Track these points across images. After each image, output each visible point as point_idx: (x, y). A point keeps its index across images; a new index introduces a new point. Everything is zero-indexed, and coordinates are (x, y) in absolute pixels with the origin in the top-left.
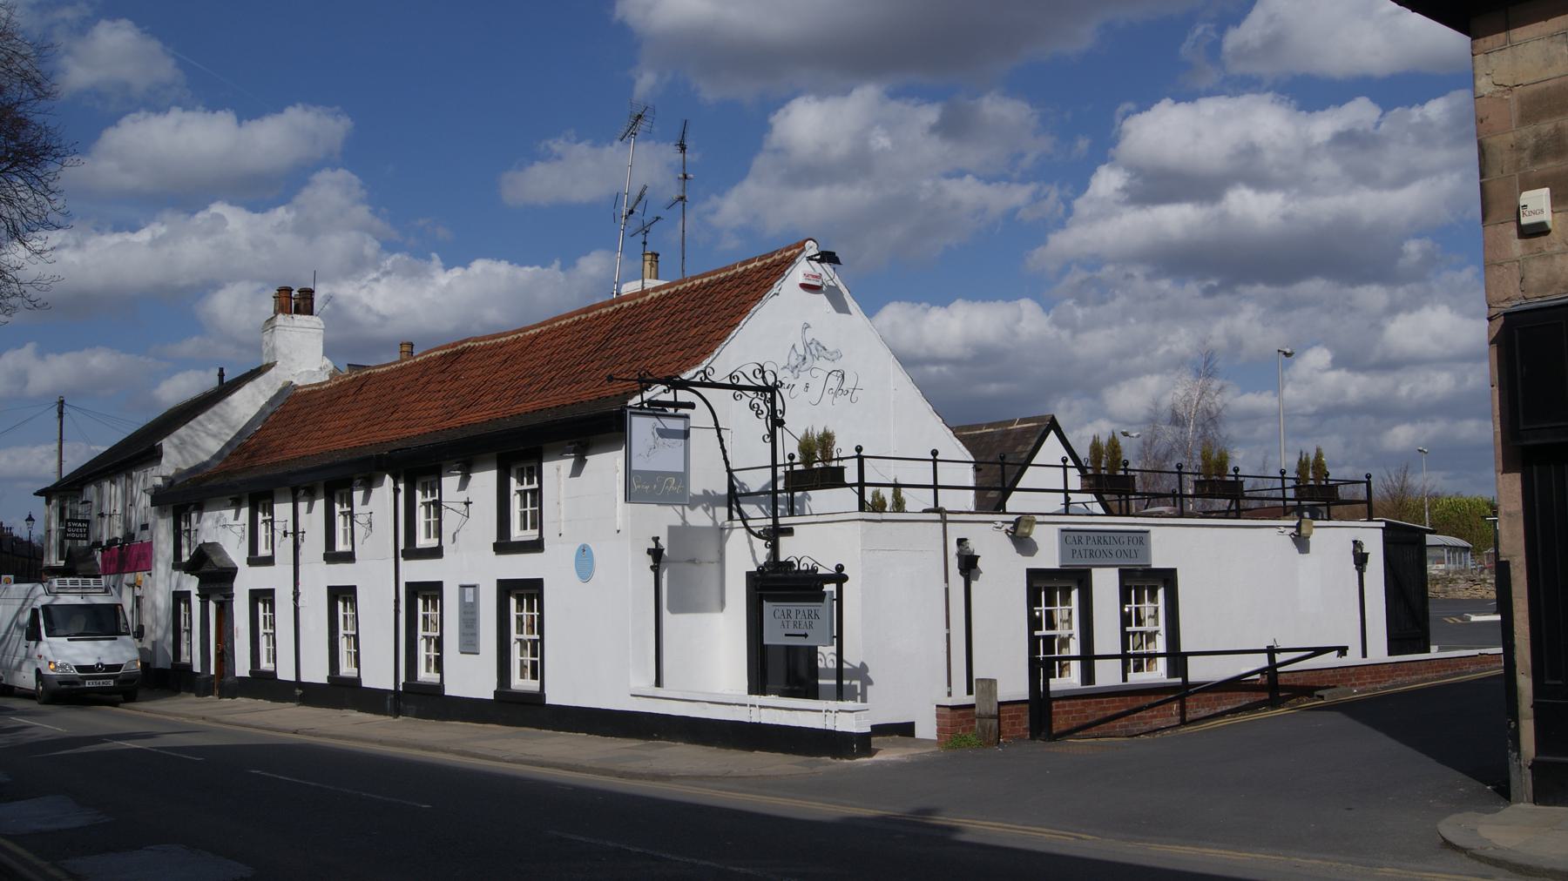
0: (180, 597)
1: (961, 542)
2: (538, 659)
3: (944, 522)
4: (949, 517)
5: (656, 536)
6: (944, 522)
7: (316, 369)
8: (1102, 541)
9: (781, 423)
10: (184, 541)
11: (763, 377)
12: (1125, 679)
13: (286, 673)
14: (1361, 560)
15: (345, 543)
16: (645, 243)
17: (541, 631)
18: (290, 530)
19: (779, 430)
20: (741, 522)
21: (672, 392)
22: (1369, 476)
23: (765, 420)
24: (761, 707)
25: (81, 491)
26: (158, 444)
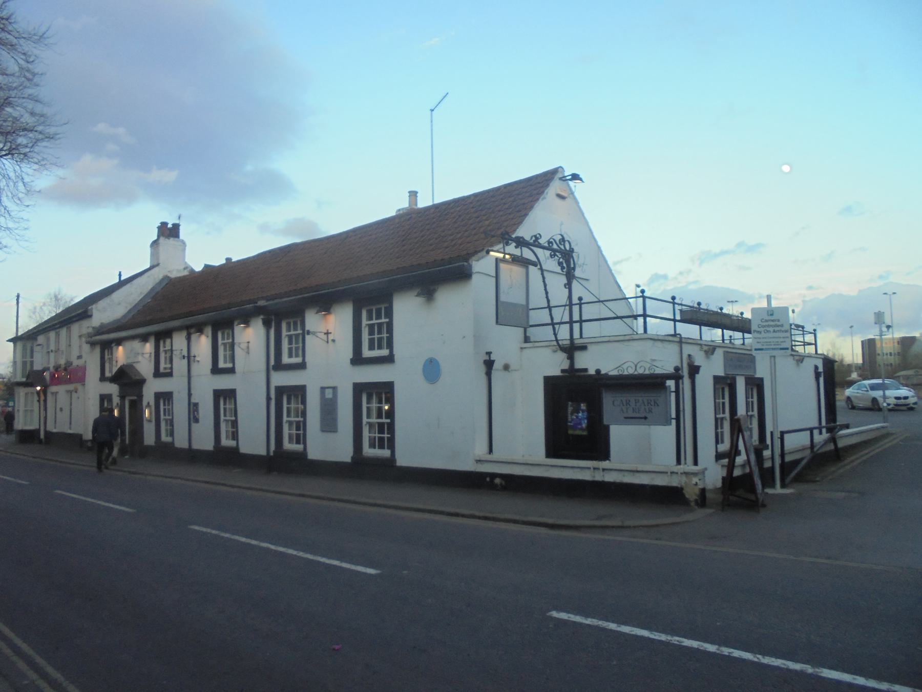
2: (301, 432)
7: (182, 267)
10: (107, 366)
13: (181, 442)
14: (817, 375)
17: (391, 414)
18: (186, 355)
20: (555, 342)
22: (815, 330)
24: (604, 470)
25: (36, 339)
26: (90, 308)
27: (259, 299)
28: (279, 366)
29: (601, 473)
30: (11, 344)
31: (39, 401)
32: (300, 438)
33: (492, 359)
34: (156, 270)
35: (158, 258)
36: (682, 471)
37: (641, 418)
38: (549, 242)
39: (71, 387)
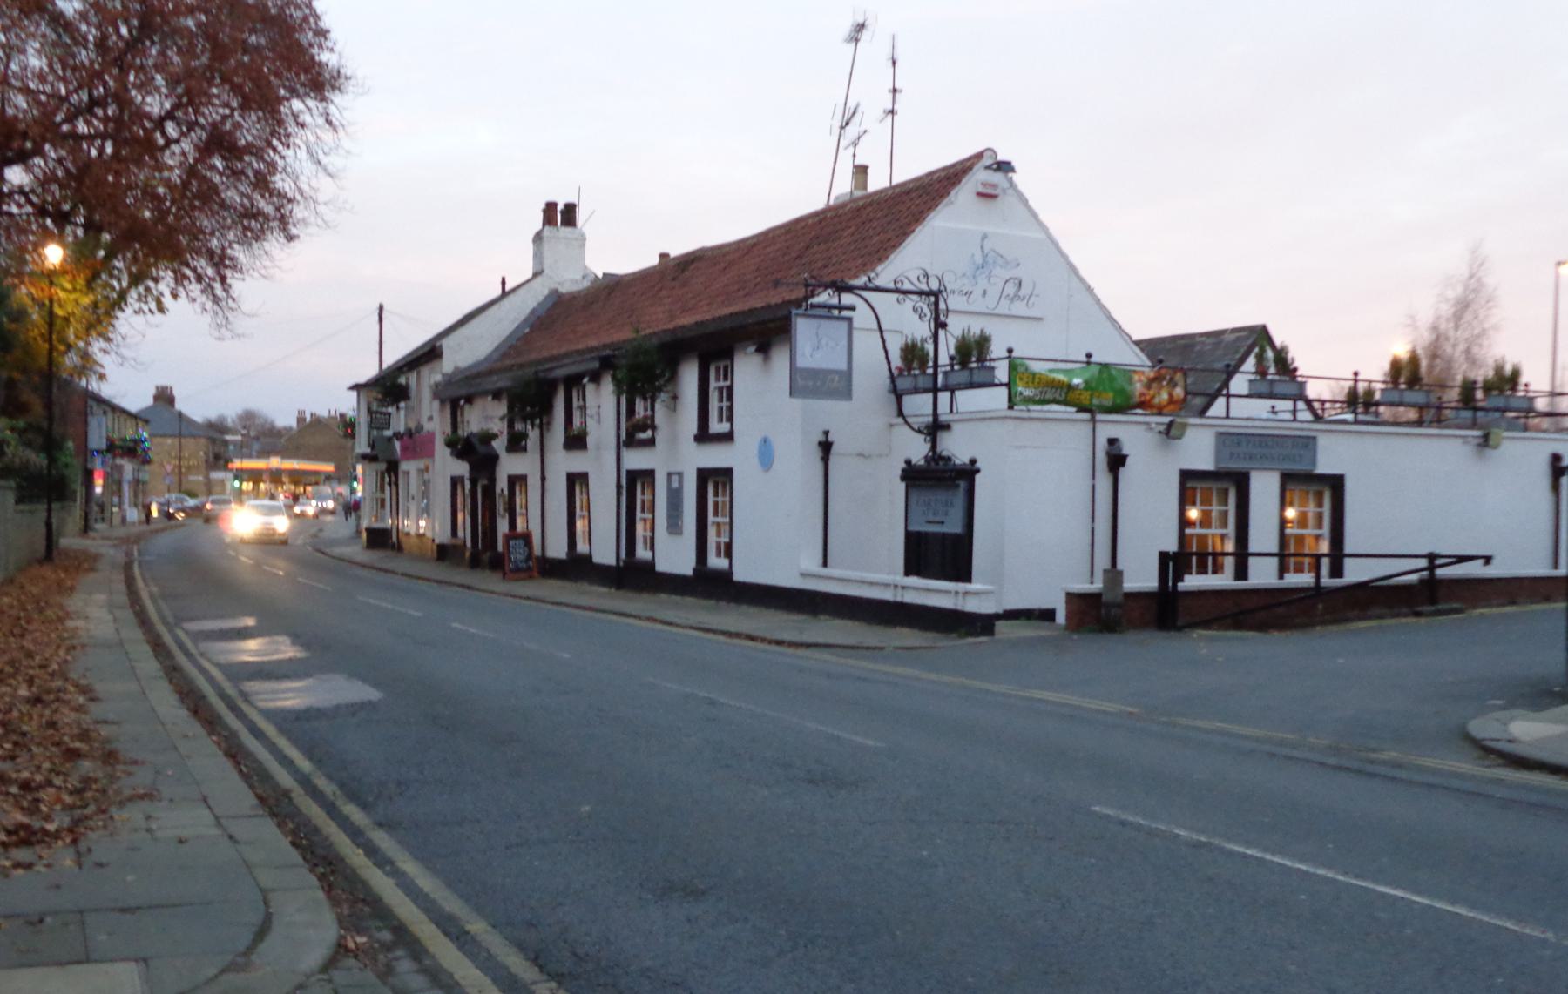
0: (456, 482)
1: (1112, 442)
3: (1093, 420)
4: (1099, 417)
5: (827, 428)
6: (1093, 420)
7: (579, 277)
8: (1264, 445)
9: (944, 326)
11: (927, 283)
12: (1281, 577)
16: (854, 155)
19: (941, 332)
23: (927, 323)
24: (903, 588)
29: (900, 591)
30: (354, 394)
31: (390, 484)
33: (830, 439)
34: (539, 280)
35: (541, 263)
36: (964, 591)
37: (938, 522)
39: (421, 464)
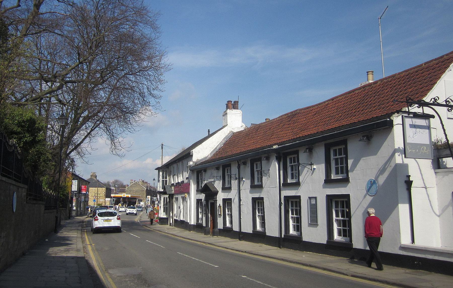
13: (236, 228)
15: (258, 181)
21: (421, 107)
27: (275, 144)
28: (286, 185)
32: (298, 228)
38: (446, 101)
